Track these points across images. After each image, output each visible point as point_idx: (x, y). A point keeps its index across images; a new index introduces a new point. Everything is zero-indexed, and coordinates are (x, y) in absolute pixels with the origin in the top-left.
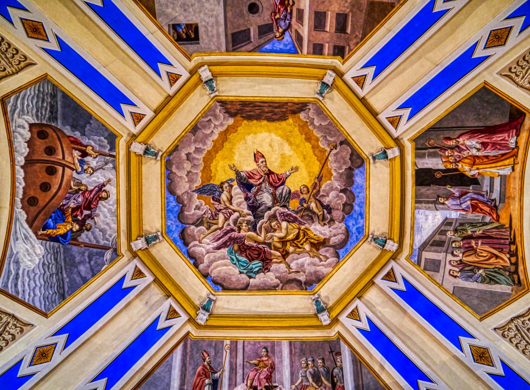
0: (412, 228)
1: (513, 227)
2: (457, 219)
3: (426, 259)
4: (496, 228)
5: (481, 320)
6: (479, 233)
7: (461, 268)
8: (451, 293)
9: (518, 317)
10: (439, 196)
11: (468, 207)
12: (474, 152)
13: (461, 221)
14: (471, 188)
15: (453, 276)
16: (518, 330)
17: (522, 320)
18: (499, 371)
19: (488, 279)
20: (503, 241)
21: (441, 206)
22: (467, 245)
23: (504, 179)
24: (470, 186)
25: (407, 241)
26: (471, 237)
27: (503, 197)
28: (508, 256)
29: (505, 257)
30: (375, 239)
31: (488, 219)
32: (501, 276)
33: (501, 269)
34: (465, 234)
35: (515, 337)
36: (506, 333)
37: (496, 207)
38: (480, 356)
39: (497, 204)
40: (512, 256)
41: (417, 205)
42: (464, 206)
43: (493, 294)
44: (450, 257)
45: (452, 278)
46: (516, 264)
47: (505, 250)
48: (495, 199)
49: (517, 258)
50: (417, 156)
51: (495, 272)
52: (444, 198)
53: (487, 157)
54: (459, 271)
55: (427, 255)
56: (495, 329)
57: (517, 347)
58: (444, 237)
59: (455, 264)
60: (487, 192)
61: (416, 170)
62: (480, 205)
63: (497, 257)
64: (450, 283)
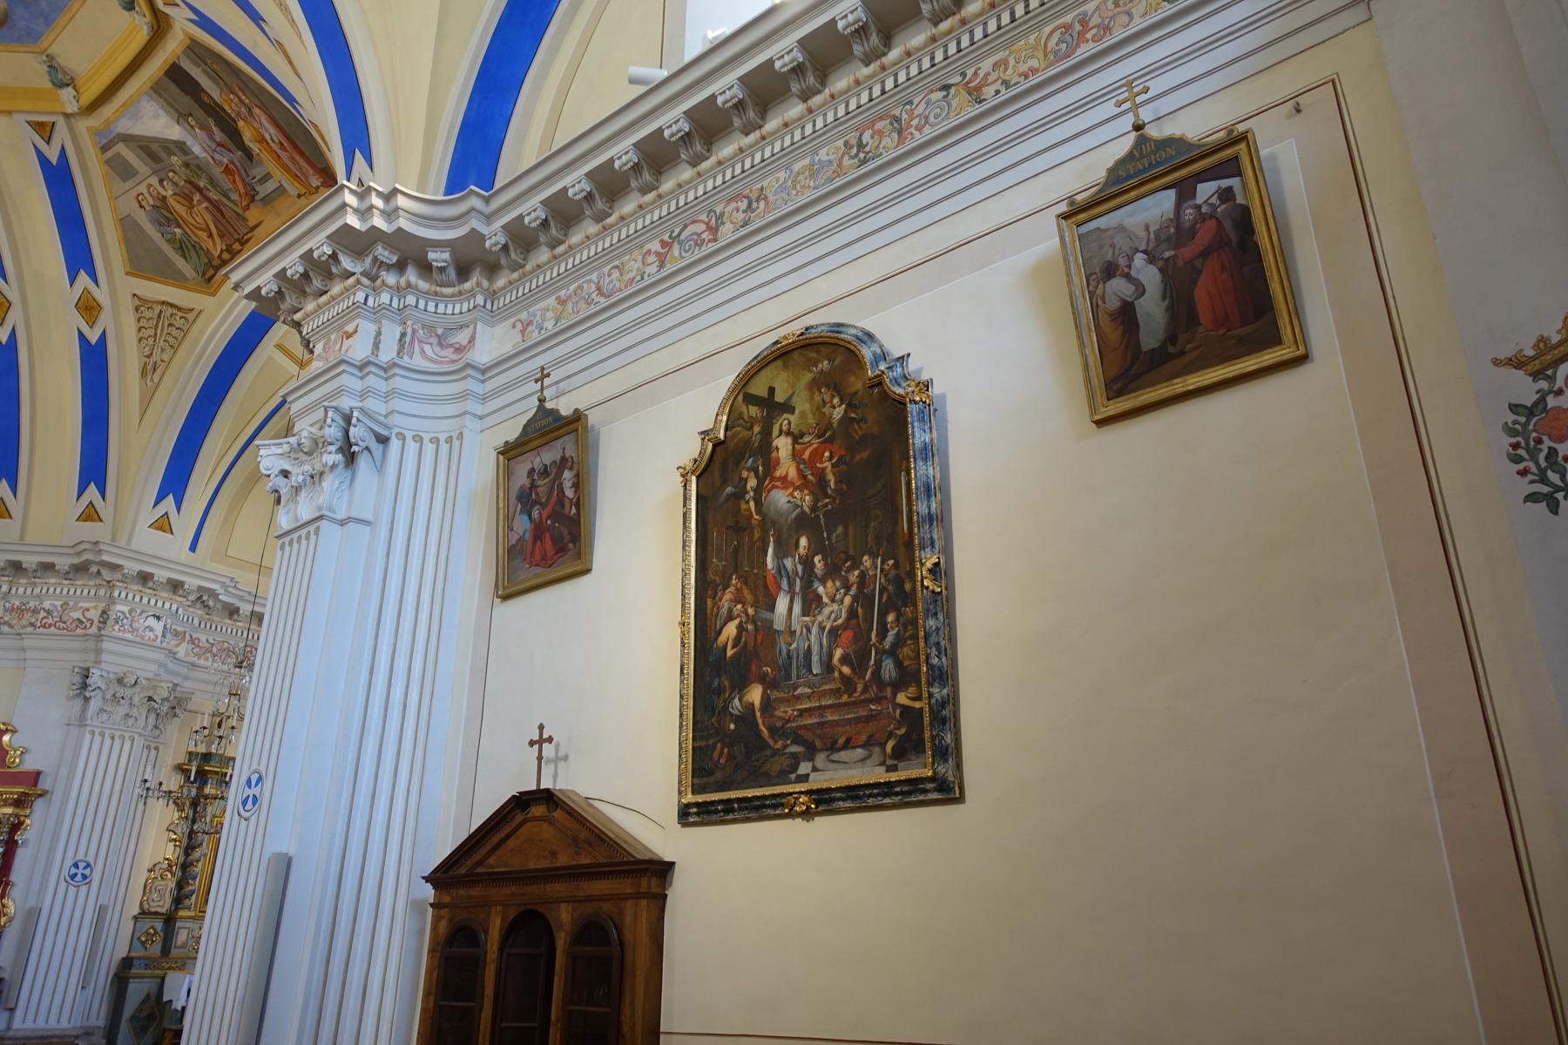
0: (125, 106)
1: (257, 231)
2: (197, 157)
3: (118, 153)
4: (236, 213)
5: (127, 273)
6: (214, 195)
7: (158, 205)
8: (120, 218)
9: (172, 305)
10: (191, 115)
11: (221, 163)
12: (267, 136)
13: (201, 165)
14: (240, 153)
15: (139, 202)
16: (159, 317)
17: (174, 312)
18: (93, 337)
19: (178, 245)
20: (232, 230)
21: (186, 125)
22: (187, 192)
23: (280, 190)
24: (240, 150)
25: (107, 111)
26: (200, 190)
27: (267, 200)
28: (224, 247)
29: (220, 246)
30: (53, 67)
31: (234, 197)
32: (196, 256)
33: (204, 250)
34: (195, 180)
35: (148, 320)
36: (142, 308)
37: (253, 198)
38: (86, 307)
39: (257, 198)
40: (227, 250)
41: (151, 92)
42: (217, 156)
43: (168, 261)
44: (154, 181)
45: (137, 205)
46: (225, 263)
47: (226, 238)
48: (258, 193)
49: (231, 259)
50: (184, 52)
51: (194, 247)
52: (197, 123)
53: (279, 157)
54: (152, 206)
55: (121, 148)
56: (134, 295)
57: (140, 330)
58: (163, 155)
59: (155, 194)
60: (255, 177)
61: (174, 62)
62: (236, 177)
63: (211, 235)
64: (129, 206)
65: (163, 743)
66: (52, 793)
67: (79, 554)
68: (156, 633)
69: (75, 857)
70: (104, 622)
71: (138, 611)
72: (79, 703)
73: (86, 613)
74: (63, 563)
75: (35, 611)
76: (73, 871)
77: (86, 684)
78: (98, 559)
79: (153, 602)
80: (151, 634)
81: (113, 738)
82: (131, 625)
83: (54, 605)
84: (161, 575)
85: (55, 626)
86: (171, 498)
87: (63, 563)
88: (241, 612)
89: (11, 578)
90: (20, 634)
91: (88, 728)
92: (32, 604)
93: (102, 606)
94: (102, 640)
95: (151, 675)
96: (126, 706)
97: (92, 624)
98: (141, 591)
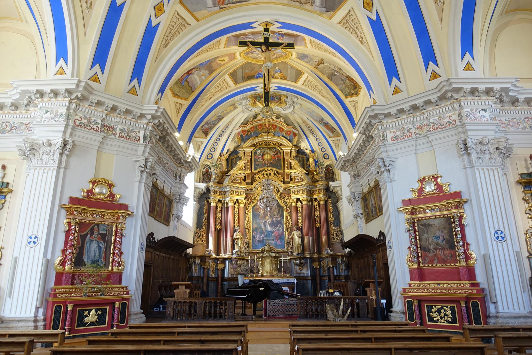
65: (508, 171)
66: (471, 200)
67: (439, 91)
68: (487, 118)
69: (494, 229)
70: (461, 119)
71: (475, 109)
72: (466, 157)
73: (451, 118)
74: (434, 98)
75: (427, 125)
76: (496, 235)
77: (467, 147)
78: (450, 88)
79: (480, 103)
80: (484, 119)
81: (488, 170)
82: (474, 117)
83: (435, 119)
84: (482, 87)
85: (439, 128)
86: (467, 54)
87: (434, 98)
88: (520, 100)
89: (413, 114)
90: (426, 136)
91: (476, 168)
92: (425, 123)
93: (457, 112)
94: (465, 126)
95: (493, 137)
96: (488, 154)
97: (456, 122)
98: (473, 99)
